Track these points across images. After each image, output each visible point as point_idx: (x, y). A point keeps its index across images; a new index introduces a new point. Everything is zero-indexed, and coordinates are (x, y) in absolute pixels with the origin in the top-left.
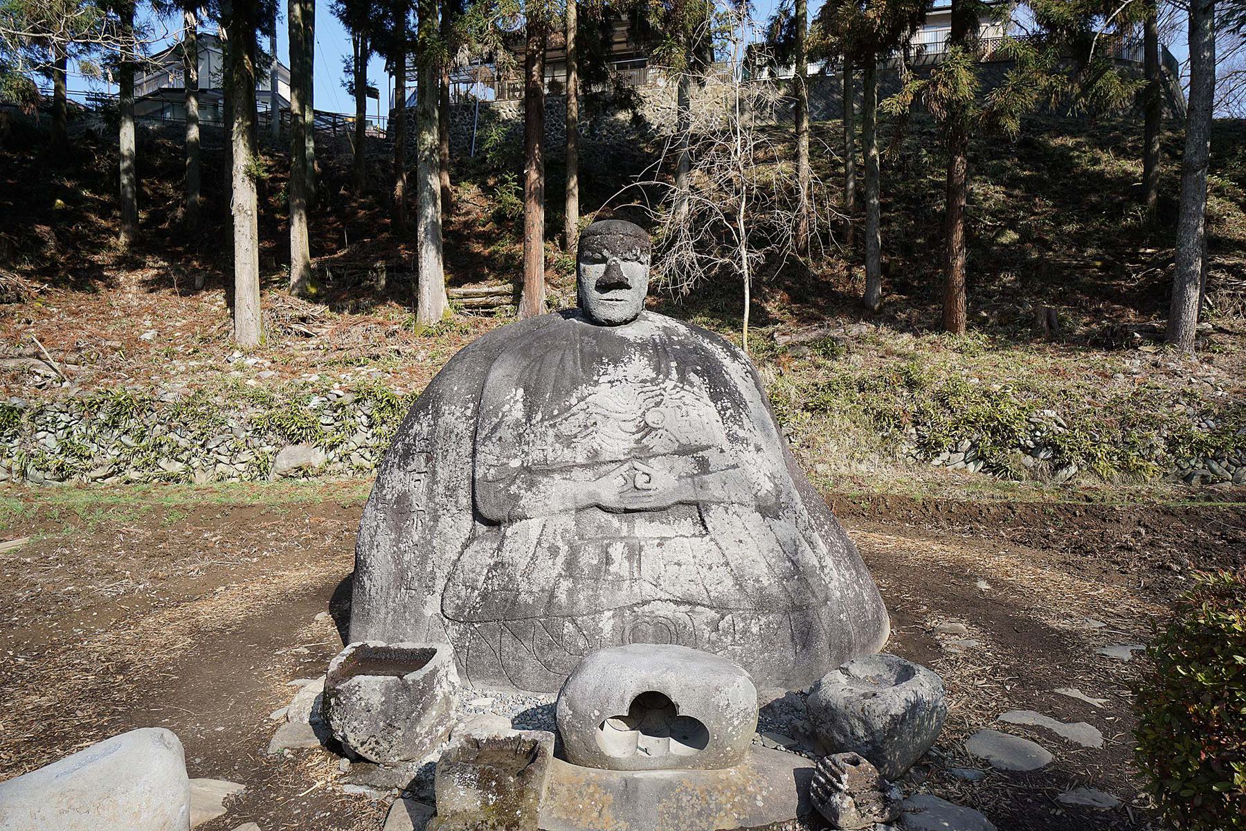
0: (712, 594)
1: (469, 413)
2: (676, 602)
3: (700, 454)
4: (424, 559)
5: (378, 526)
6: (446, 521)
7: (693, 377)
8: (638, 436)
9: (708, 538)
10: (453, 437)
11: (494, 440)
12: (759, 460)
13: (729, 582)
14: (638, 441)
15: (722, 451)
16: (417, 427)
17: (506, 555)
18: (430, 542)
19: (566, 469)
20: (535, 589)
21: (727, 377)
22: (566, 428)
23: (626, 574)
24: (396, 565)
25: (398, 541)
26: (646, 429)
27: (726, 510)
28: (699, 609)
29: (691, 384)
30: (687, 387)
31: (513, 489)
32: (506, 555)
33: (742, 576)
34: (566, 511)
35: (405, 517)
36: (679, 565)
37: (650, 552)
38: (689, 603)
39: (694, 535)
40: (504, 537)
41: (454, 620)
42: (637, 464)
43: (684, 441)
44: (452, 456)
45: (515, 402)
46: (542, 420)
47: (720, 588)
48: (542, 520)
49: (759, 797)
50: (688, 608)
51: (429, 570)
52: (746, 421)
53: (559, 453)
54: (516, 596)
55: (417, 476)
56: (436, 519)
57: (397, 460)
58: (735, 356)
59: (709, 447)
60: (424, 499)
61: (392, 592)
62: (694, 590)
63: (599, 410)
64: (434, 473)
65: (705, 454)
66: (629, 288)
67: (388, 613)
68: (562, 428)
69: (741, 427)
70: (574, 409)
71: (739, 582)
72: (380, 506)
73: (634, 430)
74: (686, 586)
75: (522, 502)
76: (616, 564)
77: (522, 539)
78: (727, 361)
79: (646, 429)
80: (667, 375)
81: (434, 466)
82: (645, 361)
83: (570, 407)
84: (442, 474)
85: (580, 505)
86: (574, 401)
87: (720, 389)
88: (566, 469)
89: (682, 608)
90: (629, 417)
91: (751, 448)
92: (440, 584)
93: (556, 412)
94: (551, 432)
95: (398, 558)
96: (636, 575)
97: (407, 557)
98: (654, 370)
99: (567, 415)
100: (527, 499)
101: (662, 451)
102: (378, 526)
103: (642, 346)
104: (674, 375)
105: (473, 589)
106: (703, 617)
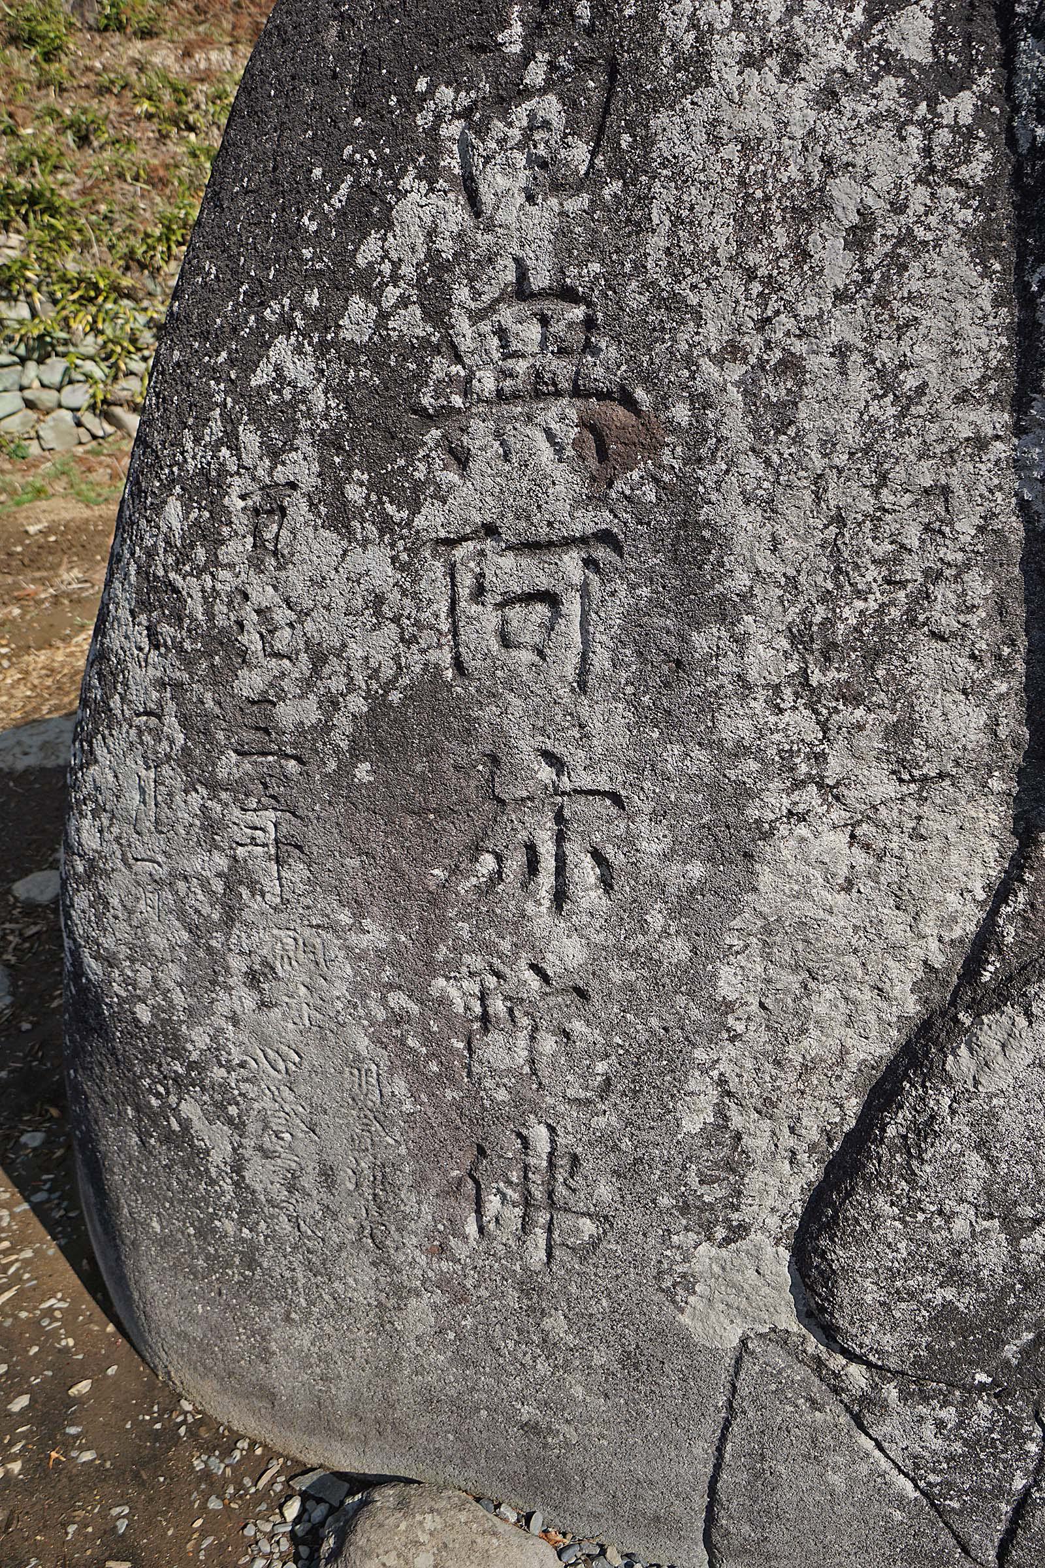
4: (647, 1075)
5: (238, 877)
6: (807, 860)
10: (836, 261)
16: (423, 211)
18: (694, 979)
24: (421, 1082)
25: (418, 967)
35: (455, 835)
41: (921, 1380)
44: (840, 403)
51: (692, 1124)
55: (509, 570)
56: (735, 845)
57: (301, 467)
60: (609, 721)
61: (422, 1210)
64: (691, 544)
67: (401, 1292)
72: (228, 765)
81: (683, 494)
84: (762, 541)
92: (777, 1193)
95: (437, 1052)
97: (503, 1052)
102: (238, 877)
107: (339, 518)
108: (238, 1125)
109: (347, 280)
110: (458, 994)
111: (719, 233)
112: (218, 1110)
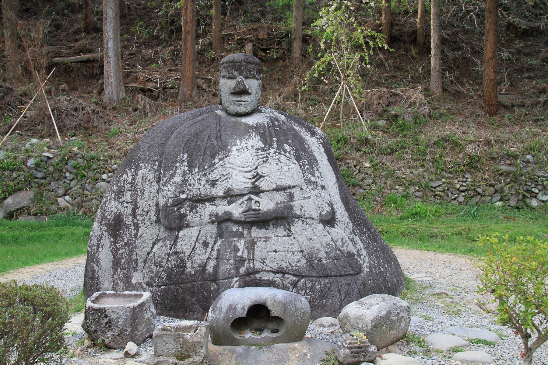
0: (294, 268)
1: (156, 167)
2: (273, 272)
3: (289, 190)
7: (286, 147)
8: (254, 180)
9: (291, 238)
11: (171, 183)
12: (323, 194)
13: (304, 261)
14: (253, 183)
15: (302, 189)
16: (125, 176)
17: (179, 248)
19: (212, 199)
20: (196, 266)
21: (307, 146)
22: (213, 176)
23: (245, 256)
25: (115, 242)
26: (258, 177)
27: (303, 221)
28: (287, 276)
29: (285, 151)
30: (282, 152)
31: (182, 211)
32: (179, 248)
33: (312, 258)
34: (212, 222)
36: (275, 251)
37: (260, 244)
38: (281, 273)
39: (285, 236)
40: (177, 237)
42: (253, 196)
43: (279, 183)
45: (183, 161)
46: (198, 172)
47: (298, 264)
48: (198, 228)
49: (308, 355)
50: (281, 275)
52: (316, 172)
53: (208, 190)
54: (184, 270)
55: (125, 205)
57: (113, 196)
58: (313, 134)
59: (294, 187)
62: (284, 265)
63: (231, 166)
65: (292, 190)
66: (250, 94)
68: (210, 176)
69: (313, 175)
70: (217, 165)
71: (309, 260)
72: (103, 223)
73: (251, 177)
74: (279, 264)
75: (188, 218)
76: (241, 251)
77: (187, 239)
78: (308, 137)
79: (258, 177)
80: (271, 146)
82: (258, 138)
83: (215, 164)
85: (220, 220)
86: (216, 160)
87: (302, 154)
88: (212, 199)
89: (277, 275)
90: (249, 169)
91: (319, 187)
93: (206, 167)
94: (203, 179)
96: (251, 258)
98: (263, 142)
99: (212, 168)
100: (190, 217)
101: (267, 189)
102: (102, 234)
103: (257, 128)
104: (275, 146)
105: (161, 267)
106: (289, 280)
107: (115, 200)
108: (98, 266)
109: (119, 181)
110: (118, 245)
111: (141, 180)
112: (97, 265)
